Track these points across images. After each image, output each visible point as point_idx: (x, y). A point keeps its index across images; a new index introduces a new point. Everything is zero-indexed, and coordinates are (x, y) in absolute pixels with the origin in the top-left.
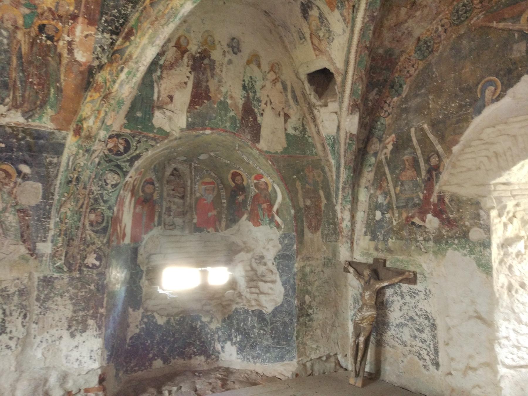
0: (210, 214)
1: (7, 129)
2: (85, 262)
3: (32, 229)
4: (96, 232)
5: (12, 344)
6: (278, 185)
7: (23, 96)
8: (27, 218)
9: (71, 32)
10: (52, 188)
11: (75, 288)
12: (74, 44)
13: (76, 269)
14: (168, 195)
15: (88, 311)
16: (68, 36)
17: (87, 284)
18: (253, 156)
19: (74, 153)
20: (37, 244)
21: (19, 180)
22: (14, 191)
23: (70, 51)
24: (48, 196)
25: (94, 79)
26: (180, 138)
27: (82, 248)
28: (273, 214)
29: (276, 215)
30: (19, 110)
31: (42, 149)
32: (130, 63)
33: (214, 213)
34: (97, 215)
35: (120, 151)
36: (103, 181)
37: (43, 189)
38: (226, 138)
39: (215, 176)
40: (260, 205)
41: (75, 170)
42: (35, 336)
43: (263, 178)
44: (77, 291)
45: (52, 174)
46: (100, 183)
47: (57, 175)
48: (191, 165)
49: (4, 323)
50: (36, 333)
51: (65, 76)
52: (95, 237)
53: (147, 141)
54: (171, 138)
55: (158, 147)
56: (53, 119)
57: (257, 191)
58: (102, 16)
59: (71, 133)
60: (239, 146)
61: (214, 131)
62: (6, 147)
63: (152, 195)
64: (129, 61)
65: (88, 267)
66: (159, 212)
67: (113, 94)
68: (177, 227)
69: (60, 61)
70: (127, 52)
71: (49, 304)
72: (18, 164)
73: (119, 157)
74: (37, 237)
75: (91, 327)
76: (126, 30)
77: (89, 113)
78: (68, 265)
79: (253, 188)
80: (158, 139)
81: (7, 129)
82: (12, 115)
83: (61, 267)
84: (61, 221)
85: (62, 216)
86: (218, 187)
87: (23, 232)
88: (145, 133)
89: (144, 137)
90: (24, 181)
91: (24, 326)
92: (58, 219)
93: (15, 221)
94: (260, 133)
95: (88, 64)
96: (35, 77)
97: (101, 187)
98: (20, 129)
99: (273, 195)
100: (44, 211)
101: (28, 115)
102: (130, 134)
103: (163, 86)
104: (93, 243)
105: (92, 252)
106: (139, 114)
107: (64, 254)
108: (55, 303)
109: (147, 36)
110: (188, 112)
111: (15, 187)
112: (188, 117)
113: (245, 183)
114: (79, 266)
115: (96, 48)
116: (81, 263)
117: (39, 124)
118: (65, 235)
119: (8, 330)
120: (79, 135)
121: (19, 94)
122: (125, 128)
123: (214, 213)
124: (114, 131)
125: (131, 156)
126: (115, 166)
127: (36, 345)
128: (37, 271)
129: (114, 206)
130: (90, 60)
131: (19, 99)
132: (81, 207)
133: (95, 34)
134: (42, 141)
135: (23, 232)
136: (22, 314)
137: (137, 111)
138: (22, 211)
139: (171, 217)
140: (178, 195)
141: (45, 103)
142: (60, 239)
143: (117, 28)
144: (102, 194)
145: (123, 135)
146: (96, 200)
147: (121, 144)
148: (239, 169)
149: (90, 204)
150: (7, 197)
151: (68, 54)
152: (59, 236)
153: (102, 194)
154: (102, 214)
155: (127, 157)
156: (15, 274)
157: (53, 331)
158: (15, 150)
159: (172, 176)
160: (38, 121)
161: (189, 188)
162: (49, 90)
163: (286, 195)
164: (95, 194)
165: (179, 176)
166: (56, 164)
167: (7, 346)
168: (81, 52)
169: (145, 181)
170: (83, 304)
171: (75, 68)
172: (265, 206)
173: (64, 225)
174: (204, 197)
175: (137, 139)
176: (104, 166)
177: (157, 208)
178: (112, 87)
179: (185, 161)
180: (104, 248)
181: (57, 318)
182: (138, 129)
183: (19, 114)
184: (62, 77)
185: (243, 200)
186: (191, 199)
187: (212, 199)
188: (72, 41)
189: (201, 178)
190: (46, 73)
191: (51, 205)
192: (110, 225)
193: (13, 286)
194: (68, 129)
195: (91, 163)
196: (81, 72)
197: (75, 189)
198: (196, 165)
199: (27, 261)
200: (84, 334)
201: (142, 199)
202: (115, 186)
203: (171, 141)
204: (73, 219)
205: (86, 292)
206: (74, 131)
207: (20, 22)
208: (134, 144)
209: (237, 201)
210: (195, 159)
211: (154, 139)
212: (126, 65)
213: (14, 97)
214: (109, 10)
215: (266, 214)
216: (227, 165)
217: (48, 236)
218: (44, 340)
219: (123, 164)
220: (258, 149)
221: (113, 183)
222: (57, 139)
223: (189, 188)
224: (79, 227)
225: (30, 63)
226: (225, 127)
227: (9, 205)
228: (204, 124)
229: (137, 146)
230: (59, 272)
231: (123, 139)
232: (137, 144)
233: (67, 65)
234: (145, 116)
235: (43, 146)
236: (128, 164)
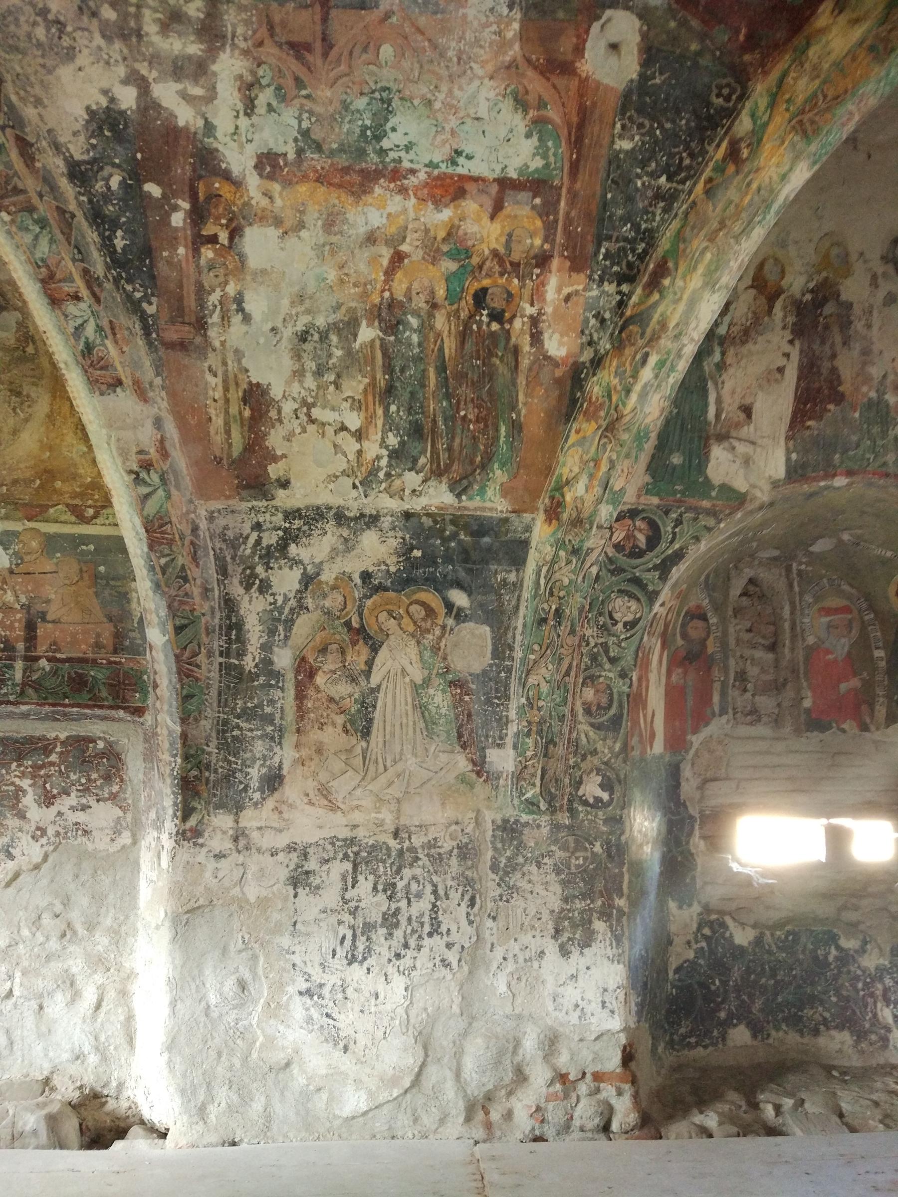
1: (424, 519)
2: (580, 793)
3: (477, 721)
4: (597, 727)
5: (452, 957)
7: (450, 449)
8: (467, 698)
9: (536, 296)
10: (510, 635)
11: (564, 848)
12: (543, 321)
13: (562, 806)
15: (592, 902)
16: (532, 305)
17: (587, 840)
19: (549, 558)
20: (487, 751)
21: (450, 622)
22: (442, 645)
23: (536, 338)
24: (504, 652)
25: (583, 393)
26: (771, 504)
27: (571, 762)
30: (445, 479)
31: (489, 555)
32: (662, 342)
34: (597, 691)
35: (638, 547)
37: (493, 638)
41: (551, 594)
42: (492, 945)
44: (568, 854)
45: (509, 607)
46: (601, 620)
47: (517, 608)
49: (436, 913)
50: (494, 939)
51: (526, 395)
52: (597, 738)
53: (695, 519)
54: (749, 507)
56: (505, 492)
58: (599, 246)
59: (541, 517)
62: (423, 556)
64: (659, 337)
65: (586, 803)
67: (628, 418)
69: (517, 361)
70: (656, 317)
71: (515, 879)
72: (448, 589)
74: (487, 736)
75: (600, 937)
76: (652, 266)
77: (576, 470)
78: (548, 798)
80: (721, 512)
81: (424, 519)
82: (431, 490)
83: (535, 801)
84: (531, 705)
85: (531, 693)
87: (461, 726)
88: (692, 501)
90: (458, 624)
91: (471, 923)
92: (523, 700)
93: (445, 703)
95: (571, 361)
96: (470, 405)
97: (604, 628)
98: (448, 518)
100: (497, 683)
101: (460, 488)
102: (658, 507)
103: (728, 386)
104: (594, 752)
105: (592, 771)
106: (676, 459)
107: (539, 772)
108: (526, 878)
109: (701, 269)
110: (788, 438)
111: (443, 635)
112: (788, 452)
114: (569, 800)
115: (586, 321)
116: (571, 794)
117: (480, 504)
118: (540, 732)
119: (444, 929)
120: (558, 519)
121: (442, 445)
122: (646, 494)
124: (625, 503)
125: (663, 556)
126: (629, 580)
127: (495, 965)
128: (489, 808)
129: (632, 671)
130: (576, 349)
131: (444, 457)
132: (567, 674)
133: (584, 290)
134: (486, 540)
135: (461, 726)
136: (467, 897)
137: (671, 452)
138: (457, 683)
141: (490, 460)
142: (530, 742)
143: (630, 265)
145: (643, 510)
146: (594, 658)
147: (640, 530)
149: (583, 667)
150: (430, 657)
151: (532, 345)
152: (528, 734)
154: (609, 687)
155: (654, 558)
156: (450, 813)
157: (526, 939)
158: (440, 561)
160: (478, 498)
162: (497, 430)
164: (592, 644)
166: (514, 584)
167: (443, 961)
168: (556, 336)
170: (581, 885)
171: (546, 375)
173: (536, 712)
175: (674, 516)
178: (624, 404)
180: (617, 763)
181: (532, 911)
182: (675, 492)
183: (444, 487)
184: (521, 397)
188: (540, 314)
190: (490, 393)
191: (509, 670)
192: (625, 712)
193: (447, 837)
194: (534, 510)
195: (584, 578)
196: (558, 382)
197: (553, 634)
198: (803, 567)
199: (472, 786)
200: (586, 951)
202: (630, 625)
203: (751, 512)
204: (554, 700)
205: (585, 859)
206: (545, 511)
207: (441, 292)
208: (669, 529)
211: (712, 513)
212: (652, 347)
213: (435, 453)
214: (614, 228)
217: (506, 734)
218: (510, 956)
221: (626, 619)
222: (515, 531)
224: (564, 716)
225: (461, 376)
226: (885, 464)
227: (435, 672)
228: (829, 462)
229: (674, 534)
230: (531, 812)
231: (644, 519)
232: (676, 526)
233: (530, 369)
234: (690, 461)
235: (489, 549)
236: (657, 574)
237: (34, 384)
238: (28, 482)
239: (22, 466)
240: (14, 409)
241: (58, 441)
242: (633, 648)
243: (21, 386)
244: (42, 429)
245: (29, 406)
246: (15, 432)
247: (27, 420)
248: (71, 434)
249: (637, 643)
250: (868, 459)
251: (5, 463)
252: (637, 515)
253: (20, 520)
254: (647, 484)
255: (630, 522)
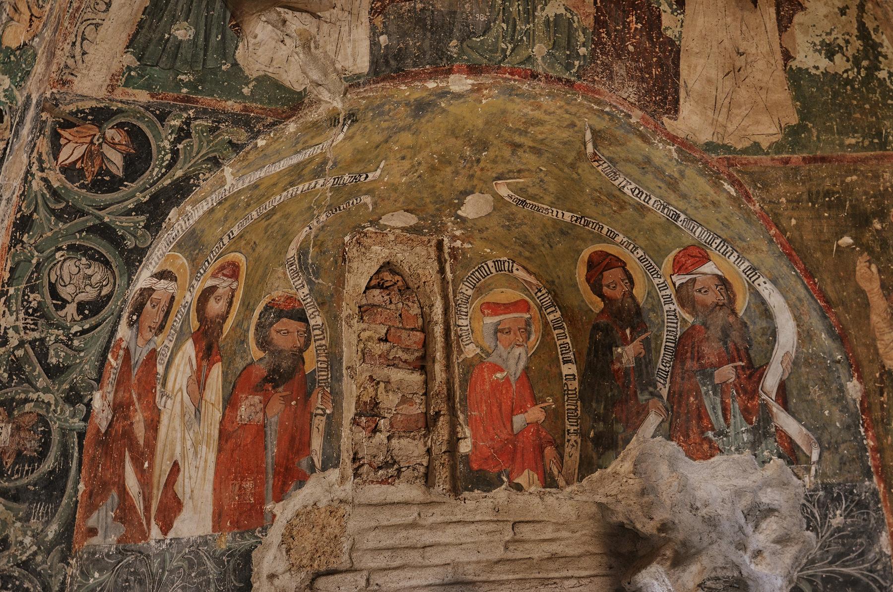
0: (519, 421)
6: (774, 282)
14: (365, 355)
18: (659, 172)
26: (352, 117)
28: (765, 406)
29: (776, 409)
33: (535, 414)
34: (18, 428)
35: (108, 172)
36: (46, 290)
38: (539, 107)
39: (531, 279)
40: (706, 373)
43: (706, 259)
46: (35, 299)
48: (440, 245)
54: (313, 115)
55: (266, 157)
57: (690, 319)
60: (596, 134)
61: (486, 79)
63: (298, 356)
66: (329, 417)
68: (406, 473)
73: (109, 197)
79: (675, 306)
80: (258, 119)
86: (543, 317)
88: (207, 101)
89: (203, 113)
94: (677, 74)
97: (38, 314)
99: (756, 327)
106: (182, 32)
113: (639, 292)
123: (535, 414)
124: (83, 97)
126: (90, 230)
129: (92, 389)
137: (174, 20)
139: (381, 437)
140: (405, 356)
144: (42, 340)
145: (120, 111)
147: (113, 145)
148: (610, 238)
153: (42, 340)
159: (377, 292)
161: (438, 330)
163: (814, 321)
164: (14, 342)
165: (406, 290)
169: (268, 308)
172: (727, 373)
174: (493, 359)
175: (176, 123)
176: (49, 234)
177: (318, 401)
179: (415, 230)
182: (178, 85)
185: (637, 359)
186: (448, 367)
187: (522, 364)
189: (479, 291)
192: (74, 465)
198: (458, 243)
201: (262, 370)
203: (316, 127)
209: (616, 366)
210: (449, 222)
211: (242, 120)
215: (735, 407)
216: (564, 230)
219: (122, 223)
220: (673, 139)
221: (82, 297)
223: (438, 330)
228: (441, 53)
229: (175, 153)
231: (120, 126)
232: (178, 140)
234: (207, 39)
242: (95, 350)
249: (102, 341)
250: (504, 51)
252: (106, 120)
254: (129, 68)
255: (95, 130)
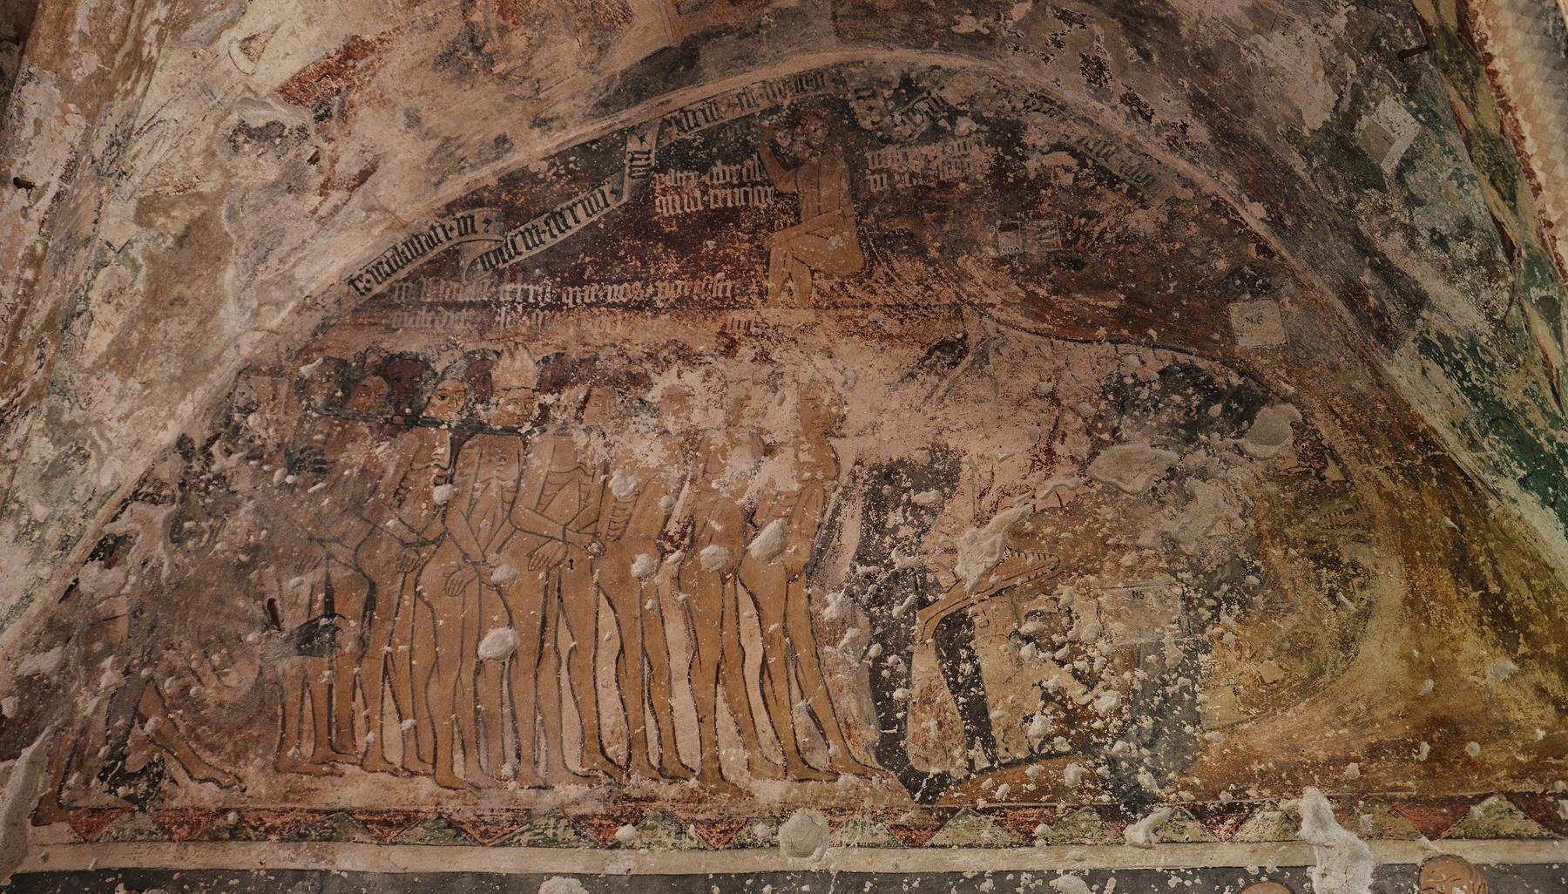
237: (1359, 539)
238: (1405, 748)
239: (1380, 713)
240: (1332, 595)
241: (1446, 654)
243: (1333, 547)
244: (1405, 631)
245: (1363, 587)
246: (1346, 642)
247: (1365, 615)
248: (1472, 636)
251: (1341, 711)
253: (1411, 837)
